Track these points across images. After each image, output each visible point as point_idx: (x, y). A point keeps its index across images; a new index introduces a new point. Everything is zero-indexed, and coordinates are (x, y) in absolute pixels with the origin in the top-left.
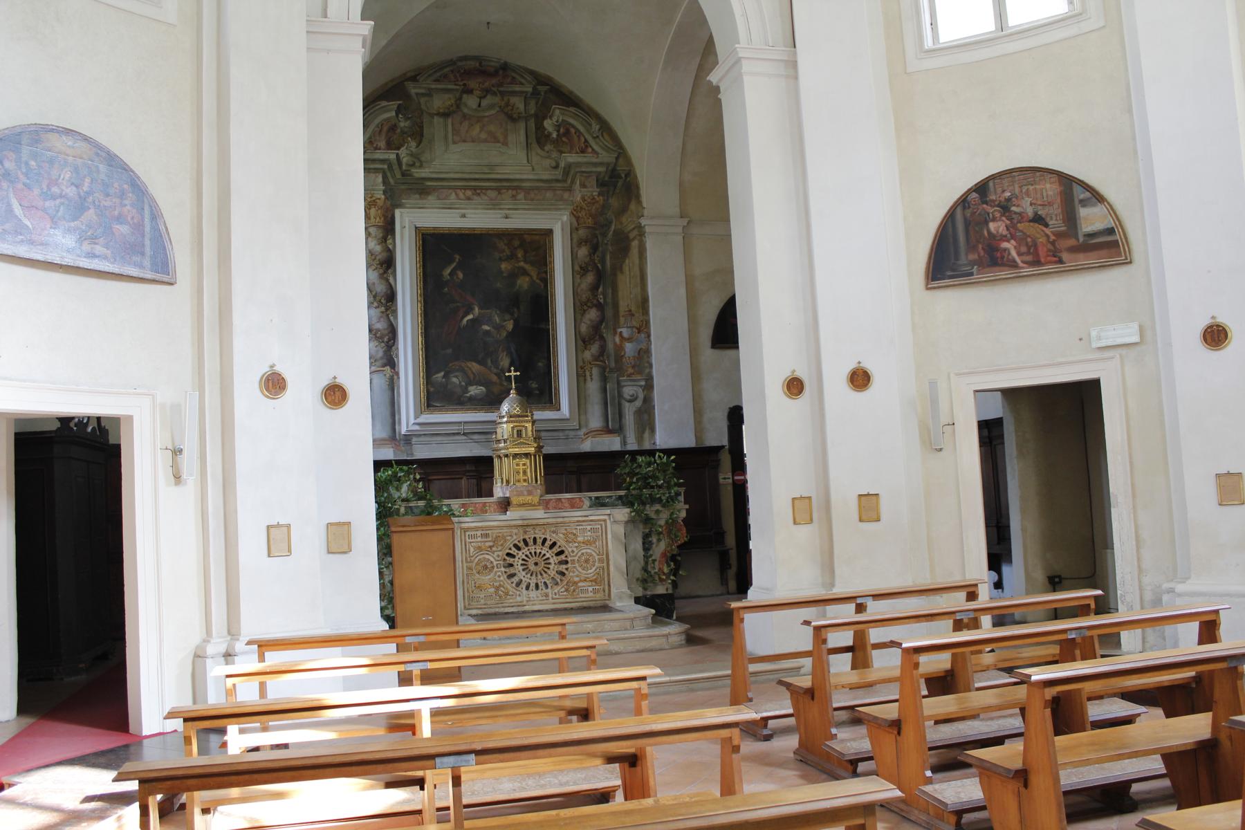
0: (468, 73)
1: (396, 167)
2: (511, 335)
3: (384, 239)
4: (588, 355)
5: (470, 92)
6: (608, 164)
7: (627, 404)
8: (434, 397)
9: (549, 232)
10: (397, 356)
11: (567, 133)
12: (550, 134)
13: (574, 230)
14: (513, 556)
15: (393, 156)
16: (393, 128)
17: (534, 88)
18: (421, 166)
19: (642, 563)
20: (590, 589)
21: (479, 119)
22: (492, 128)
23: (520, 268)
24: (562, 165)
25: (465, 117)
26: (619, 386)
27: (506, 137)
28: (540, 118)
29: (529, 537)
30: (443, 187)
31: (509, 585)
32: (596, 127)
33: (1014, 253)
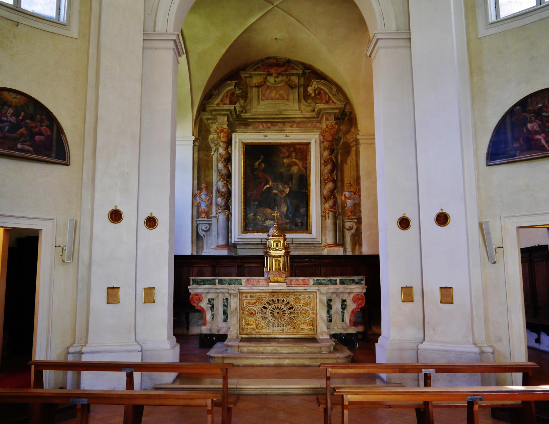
0: (271, 66)
1: (233, 113)
4: (327, 206)
5: (271, 75)
6: (340, 109)
7: (347, 231)
10: (231, 205)
11: (320, 93)
12: (311, 94)
13: (321, 142)
14: (266, 308)
15: (232, 108)
16: (233, 94)
17: (303, 72)
18: (246, 112)
19: (341, 316)
20: (307, 328)
21: (275, 88)
22: (281, 92)
23: (293, 162)
24: (317, 109)
25: (268, 87)
26: (343, 222)
28: (305, 87)
29: (275, 298)
30: (256, 122)
31: (263, 324)
32: (334, 89)
33: (543, 142)
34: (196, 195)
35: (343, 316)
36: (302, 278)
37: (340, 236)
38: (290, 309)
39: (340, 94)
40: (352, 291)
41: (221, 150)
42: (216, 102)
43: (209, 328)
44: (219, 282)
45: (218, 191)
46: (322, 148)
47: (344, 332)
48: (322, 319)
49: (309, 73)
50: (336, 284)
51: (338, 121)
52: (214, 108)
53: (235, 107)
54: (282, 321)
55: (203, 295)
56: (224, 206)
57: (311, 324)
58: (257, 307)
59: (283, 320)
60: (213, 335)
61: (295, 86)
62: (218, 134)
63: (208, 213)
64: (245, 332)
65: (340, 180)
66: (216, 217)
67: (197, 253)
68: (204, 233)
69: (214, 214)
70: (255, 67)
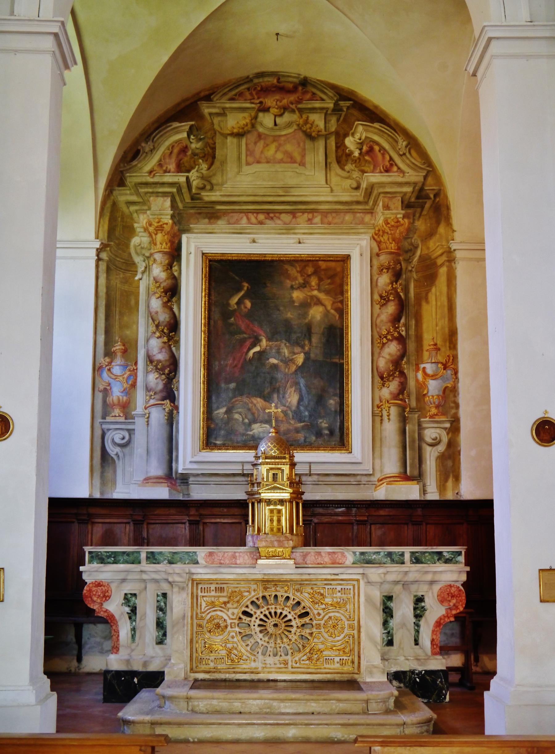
0: (266, 91)
1: (185, 190)
2: (301, 369)
3: (170, 266)
4: (386, 393)
5: (266, 110)
6: (415, 184)
8: (213, 436)
9: (346, 259)
10: (178, 389)
11: (371, 150)
12: (351, 153)
13: (374, 256)
14: (250, 615)
15: (183, 180)
16: (184, 150)
17: (336, 104)
18: (212, 189)
19: (413, 632)
20: (337, 659)
21: (276, 138)
22: (289, 147)
23: (312, 297)
24: (364, 185)
25: (260, 136)
26: (421, 428)
27: (303, 156)
28: (340, 136)
30: (234, 211)
32: (402, 143)
34: (101, 368)
35: (418, 631)
36: (328, 549)
37: (412, 459)
38: (301, 616)
39: (413, 152)
40: (437, 578)
41: (158, 271)
42: (148, 168)
43: (126, 657)
44: (148, 558)
45: (150, 359)
46: (375, 268)
47: (420, 668)
48: (371, 639)
49: (348, 108)
50: (403, 563)
51: (410, 211)
52: (144, 180)
53: (187, 178)
54: (285, 644)
55: (113, 586)
56: (161, 391)
57: (347, 650)
58: (229, 613)
59: (285, 640)
60: (133, 673)
61: (319, 136)
62: (151, 236)
63: (126, 407)
64: (203, 667)
65: (413, 338)
66: (143, 415)
67: (102, 493)
68: (118, 449)
69: (139, 408)
70: (234, 93)
